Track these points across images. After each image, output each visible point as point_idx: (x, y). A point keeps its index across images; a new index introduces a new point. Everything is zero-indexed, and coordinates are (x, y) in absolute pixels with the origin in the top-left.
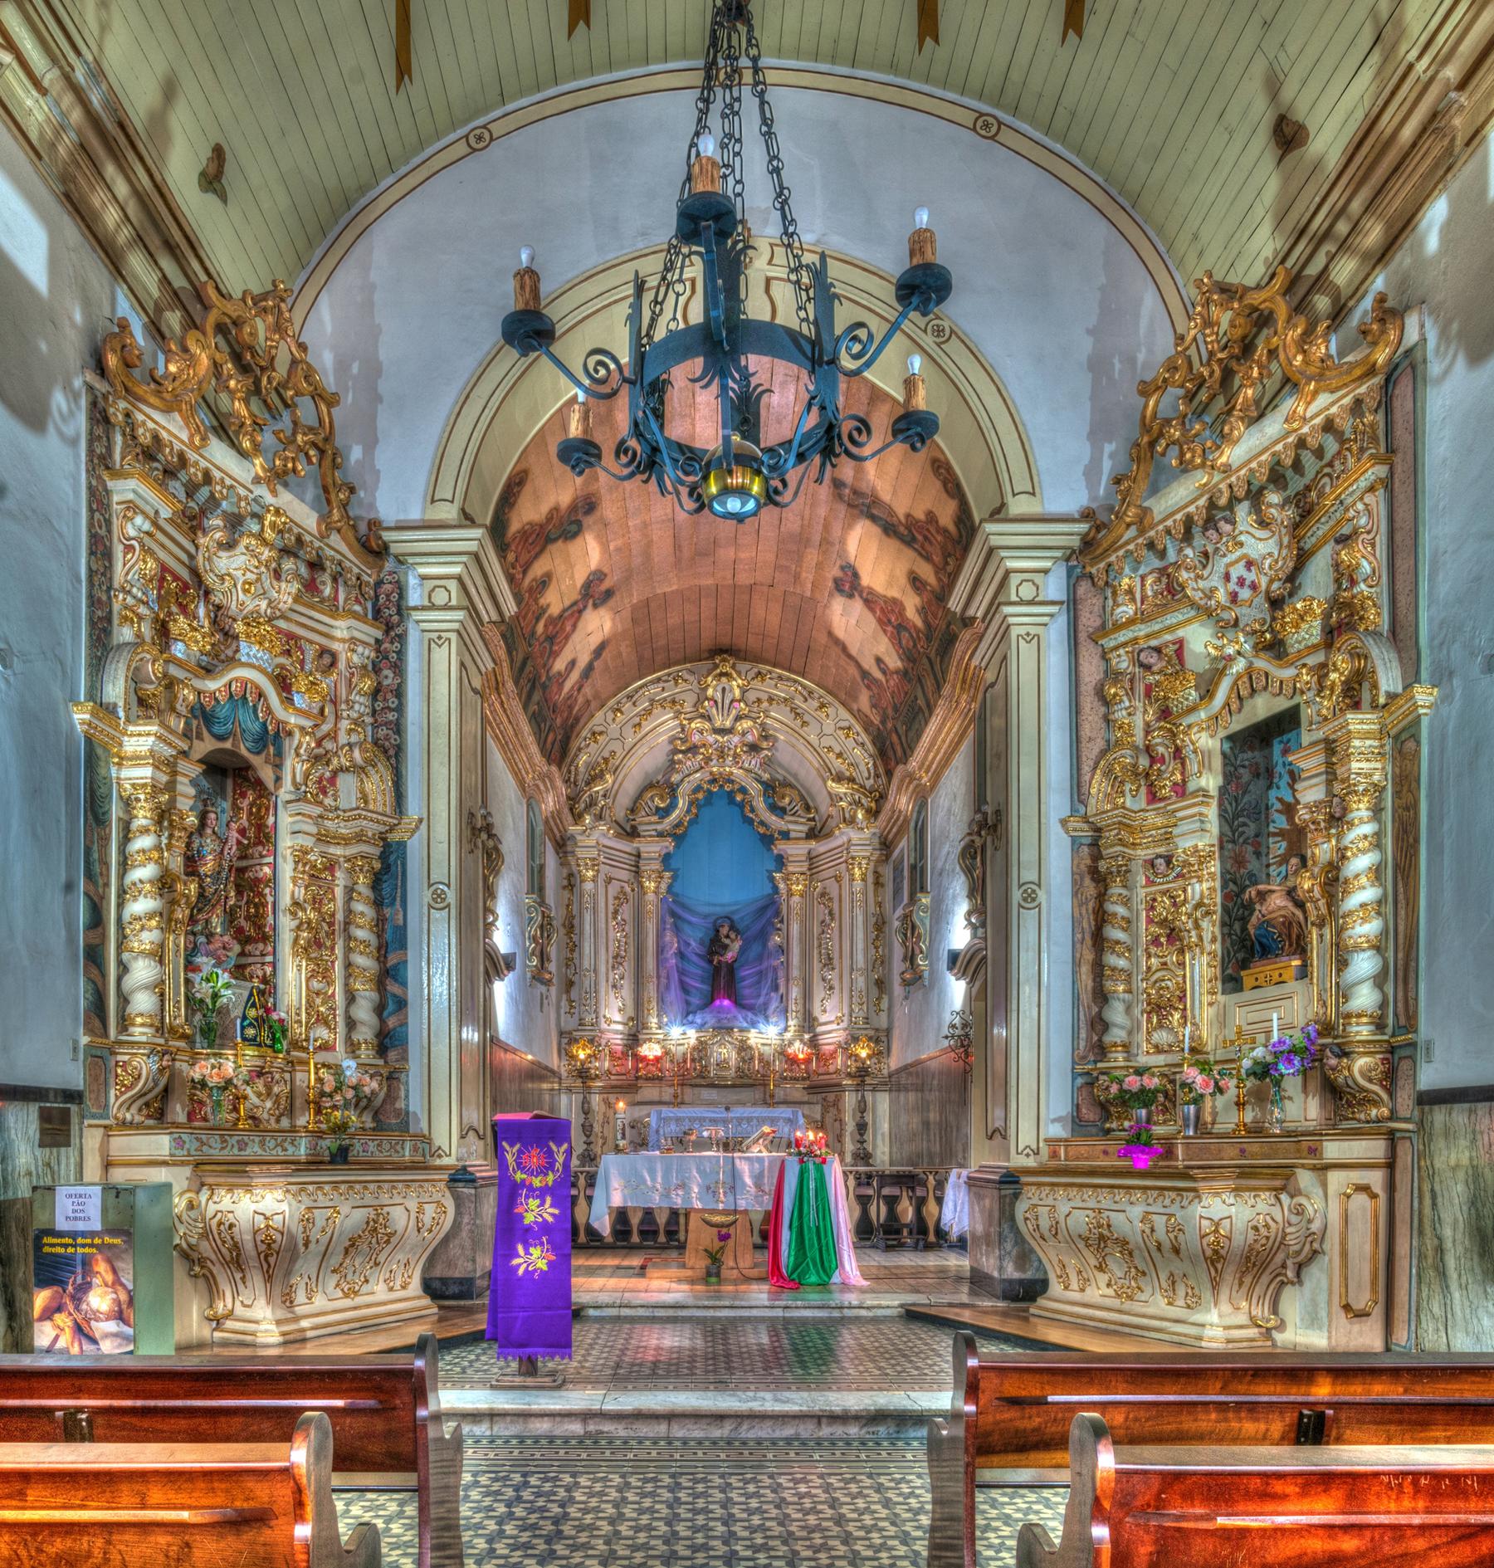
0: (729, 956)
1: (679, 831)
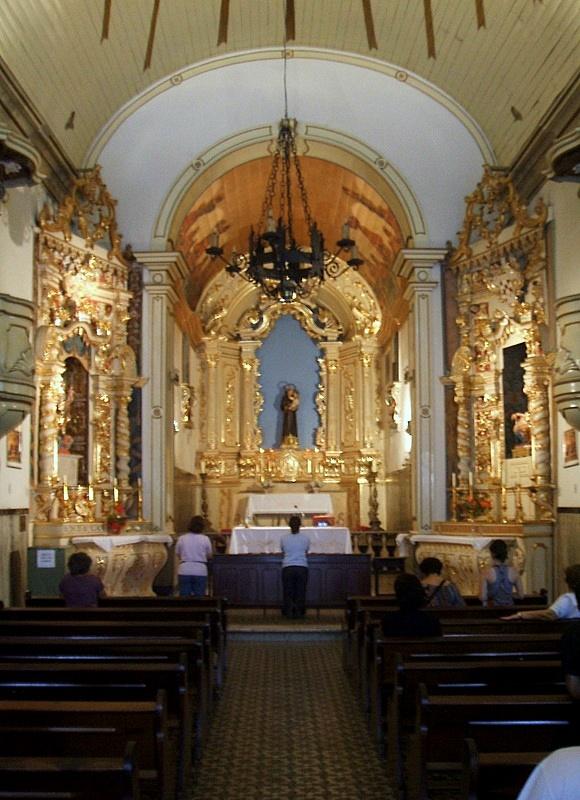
0: (293, 405)
1: (265, 336)
